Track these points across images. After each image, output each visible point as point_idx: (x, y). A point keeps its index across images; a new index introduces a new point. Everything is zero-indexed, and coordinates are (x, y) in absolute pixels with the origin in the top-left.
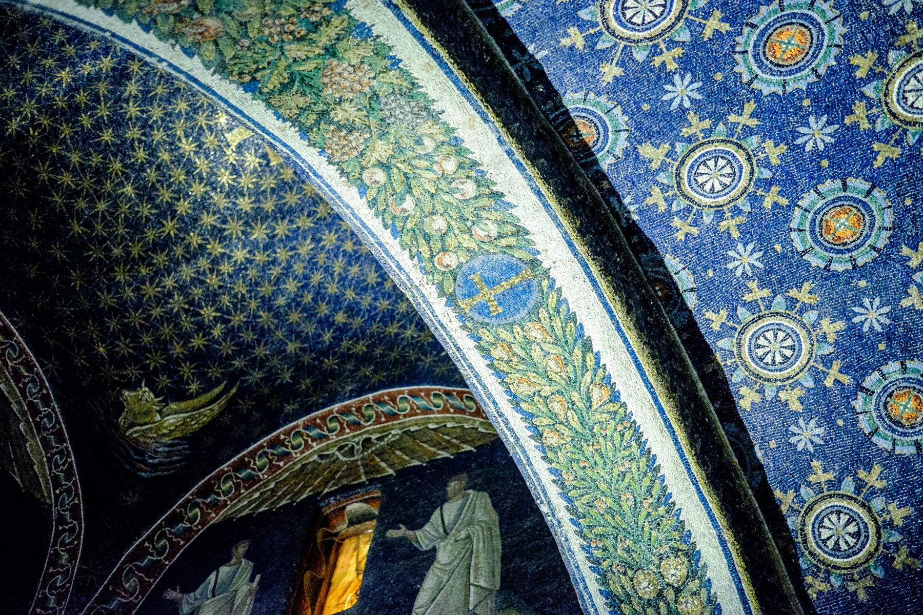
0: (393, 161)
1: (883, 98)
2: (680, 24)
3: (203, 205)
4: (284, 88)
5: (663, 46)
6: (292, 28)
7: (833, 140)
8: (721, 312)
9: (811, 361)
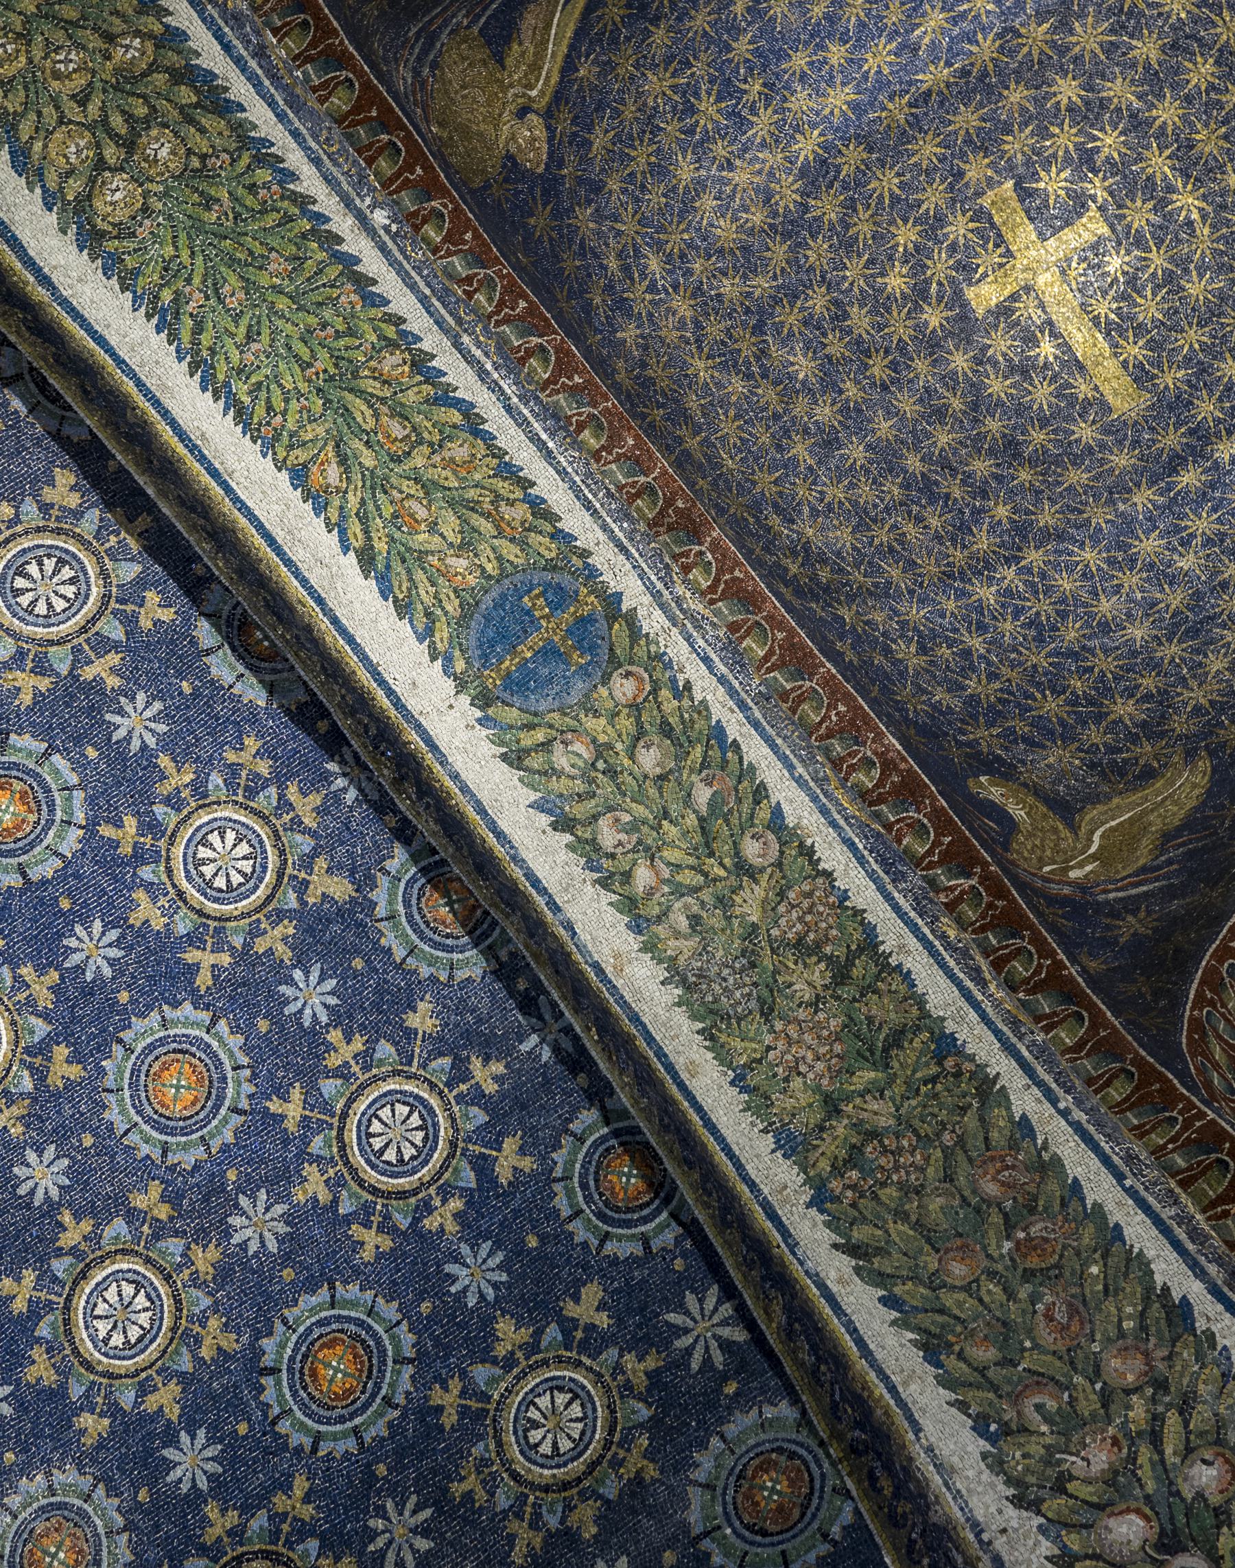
0: (733, 881)
2: (339, 1106)
3: (1155, 82)
4: (897, 1038)
5: (355, 1069)
6: (883, 1161)
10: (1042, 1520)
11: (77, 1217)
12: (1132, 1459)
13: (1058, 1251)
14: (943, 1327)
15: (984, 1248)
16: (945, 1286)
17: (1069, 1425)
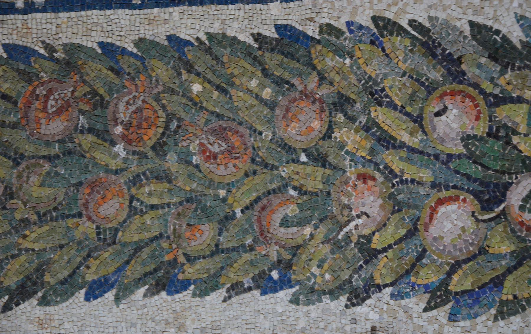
10: (388, 290)
12: (390, 173)
13: (157, 108)
14: (153, 256)
15: (108, 171)
16: (117, 230)
17: (317, 206)
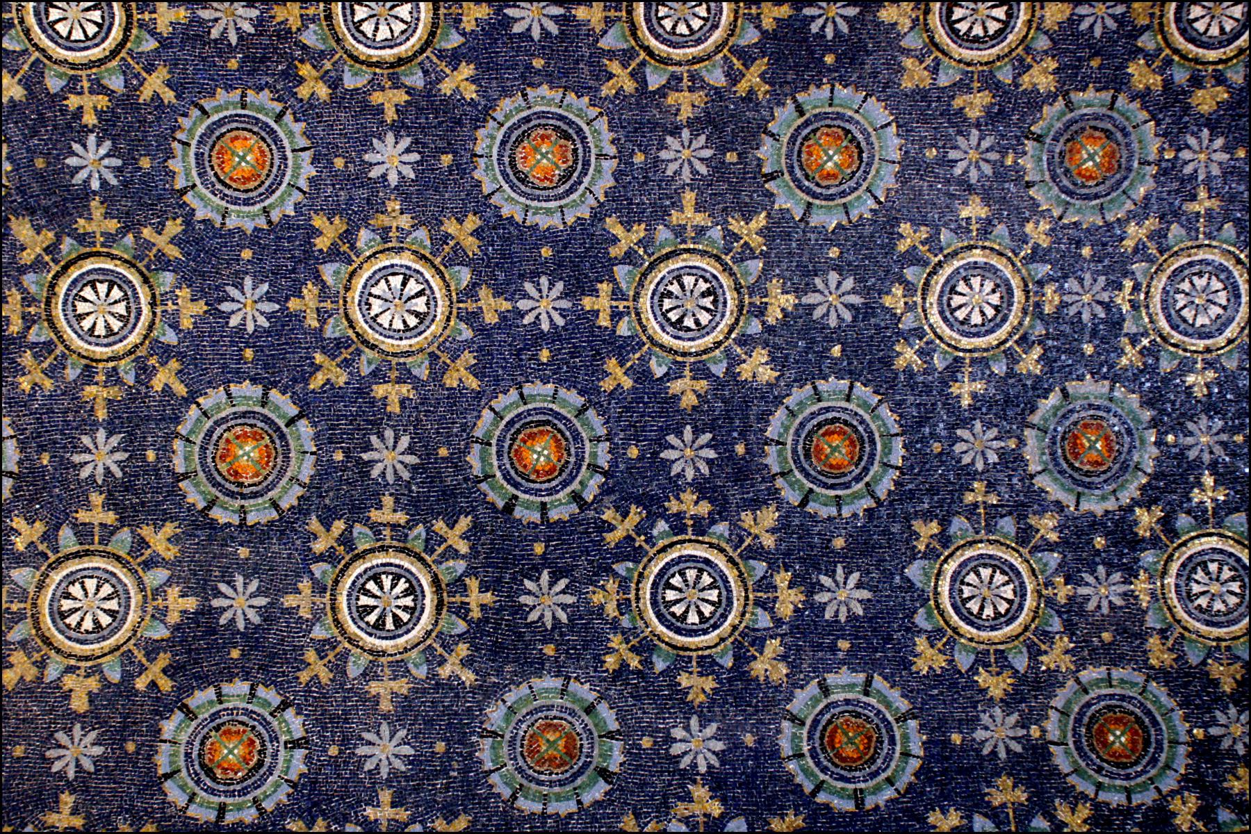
1: (342, 292)
2: (114, 63)
5: (86, 84)
7: (267, 325)
8: (37, 524)
9: (132, 642)
11: (380, 110)
